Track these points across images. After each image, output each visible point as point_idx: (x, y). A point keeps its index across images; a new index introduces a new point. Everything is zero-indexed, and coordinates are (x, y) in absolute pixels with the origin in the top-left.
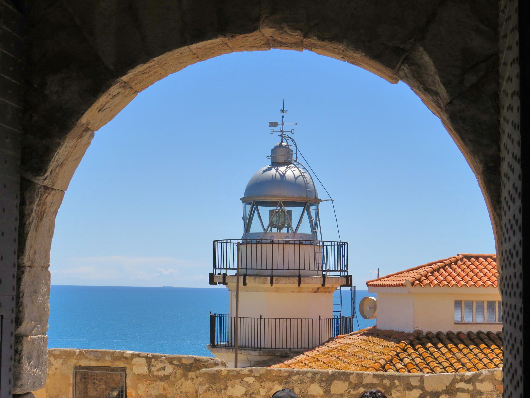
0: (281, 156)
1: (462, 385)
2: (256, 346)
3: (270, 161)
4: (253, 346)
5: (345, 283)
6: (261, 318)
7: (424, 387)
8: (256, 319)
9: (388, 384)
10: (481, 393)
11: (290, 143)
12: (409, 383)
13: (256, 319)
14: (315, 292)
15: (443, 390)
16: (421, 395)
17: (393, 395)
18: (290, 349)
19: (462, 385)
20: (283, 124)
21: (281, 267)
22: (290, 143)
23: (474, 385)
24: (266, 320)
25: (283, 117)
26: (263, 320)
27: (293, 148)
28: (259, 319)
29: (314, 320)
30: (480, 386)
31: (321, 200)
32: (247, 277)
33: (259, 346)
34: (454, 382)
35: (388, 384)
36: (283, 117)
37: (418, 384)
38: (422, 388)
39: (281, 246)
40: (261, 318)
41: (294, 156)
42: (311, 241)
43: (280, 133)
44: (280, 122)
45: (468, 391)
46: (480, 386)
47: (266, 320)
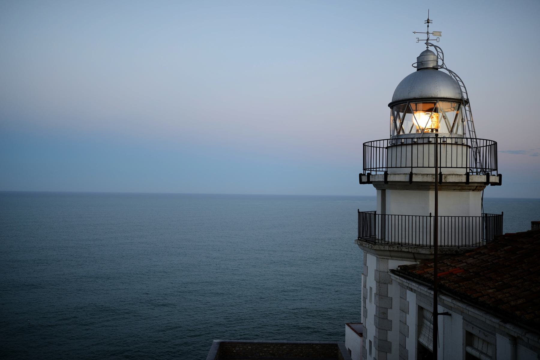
3: (416, 69)
8: (425, 218)
13: (425, 218)
14: (473, 190)
18: (459, 247)
21: (449, 165)
25: (428, 26)
32: (414, 175)
36: (428, 26)
40: (430, 216)
41: (440, 63)
43: (426, 41)
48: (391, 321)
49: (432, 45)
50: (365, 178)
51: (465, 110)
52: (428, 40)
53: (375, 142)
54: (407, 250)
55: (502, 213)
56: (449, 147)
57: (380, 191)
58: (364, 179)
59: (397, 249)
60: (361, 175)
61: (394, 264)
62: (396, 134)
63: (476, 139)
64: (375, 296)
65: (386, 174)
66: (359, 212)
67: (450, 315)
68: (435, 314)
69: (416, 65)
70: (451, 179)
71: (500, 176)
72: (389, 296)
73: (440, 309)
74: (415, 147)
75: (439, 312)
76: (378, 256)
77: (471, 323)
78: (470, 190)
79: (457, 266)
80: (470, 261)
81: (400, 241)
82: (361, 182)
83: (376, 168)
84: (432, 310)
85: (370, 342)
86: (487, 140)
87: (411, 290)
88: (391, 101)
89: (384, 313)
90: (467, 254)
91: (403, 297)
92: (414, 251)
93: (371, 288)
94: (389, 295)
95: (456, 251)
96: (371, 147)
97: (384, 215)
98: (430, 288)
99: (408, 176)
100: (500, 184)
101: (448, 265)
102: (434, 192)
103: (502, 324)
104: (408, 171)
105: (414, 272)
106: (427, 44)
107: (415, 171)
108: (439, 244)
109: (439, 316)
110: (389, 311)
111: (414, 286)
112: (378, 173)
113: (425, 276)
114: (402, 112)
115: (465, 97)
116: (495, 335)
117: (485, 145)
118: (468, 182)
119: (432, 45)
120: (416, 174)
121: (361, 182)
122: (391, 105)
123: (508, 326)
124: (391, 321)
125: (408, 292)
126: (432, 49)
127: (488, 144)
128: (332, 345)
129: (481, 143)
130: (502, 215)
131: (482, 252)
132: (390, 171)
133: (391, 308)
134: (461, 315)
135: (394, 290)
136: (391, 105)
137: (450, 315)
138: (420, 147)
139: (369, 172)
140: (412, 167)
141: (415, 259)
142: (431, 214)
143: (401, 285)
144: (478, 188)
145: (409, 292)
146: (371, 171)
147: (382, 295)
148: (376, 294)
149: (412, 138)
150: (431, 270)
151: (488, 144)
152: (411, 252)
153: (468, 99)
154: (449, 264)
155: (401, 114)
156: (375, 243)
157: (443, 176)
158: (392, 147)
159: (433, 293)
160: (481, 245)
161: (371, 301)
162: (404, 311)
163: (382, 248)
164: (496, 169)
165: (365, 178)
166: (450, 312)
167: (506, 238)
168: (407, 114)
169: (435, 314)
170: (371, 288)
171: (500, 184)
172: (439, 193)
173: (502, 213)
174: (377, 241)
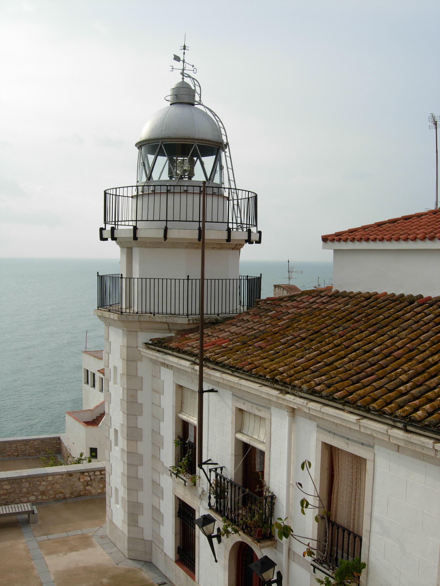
0: (184, 96)
2: (173, 312)
4: (169, 311)
6: (188, 279)
8: (182, 281)
13: (182, 281)
14: (233, 249)
20: (184, 61)
24: (194, 281)
26: (190, 281)
28: (186, 281)
32: (169, 231)
33: (185, 312)
40: (188, 279)
41: (197, 98)
43: (181, 71)
44: (182, 59)
47: (194, 281)
48: (142, 404)
49: (189, 76)
50: (108, 234)
51: (226, 156)
52: (183, 70)
53: (109, 190)
54: (160, 320)
55: (261, 275)
57: (125, 250)
58: (106, 234)
59: (148, 320)
60: (101, 230)
61: (145, 337)
62: (144, 179)
63: (236, 189)
64: (121, 377)
65: (135, 228)
66: (98, 275)
67: (217, 391)
68: (201, 392)
69: (169, 98)
71: (260, 233)
72: (138, 375)
73: (206, 387)
74: (170, 196)
75: (204, 389)
76: (125, 329)
77: (241, 398)
78: (229, 248)
79: (220, 336)
80: (233, 329)
81: (152, 311)
82: (102, 239)
83: (118, 221)
84: (196, 389)
85: (116, 431)
86: (249, 192)
87: (167, 366)
89: (132, 396)
90: (229, 322)
91: (156, 376)
92: (170, 320)
93: (115, 368)
94: (139, 374)
95: (216, 319)
96: (116, 195)
97: (130, 279)
98: (194, 363)
99: (162, 232)
100: (259, 242)
101: (209, 336)
102: (200, 251)
103: (281, 396)
105: (171, 345)
106: (183, 74)
108: (205, 312)
109: (205, 395)
110: (139, 393)
111: (172, 360)
112: (120, 227)
113: (186, 349)
114: (152, 153)
115: (225, 141)
116: (269, 409)
117: (247, 197)
118: (229, 240)
119: (189, 76)
121: (102, 239)
122: (140, 145)
123: (288, 397)
124: (142, 404)
125: (163, 369)
126: (187, 80)
127: (250, 196)
128: (54, 438)
129: (241, 195)
130: (261, 277)
131: (245, 318)
132: (140, 225)
133: (141, 389)
134: (230, 391)
135: (143, 369)
137: (217, 391)
138: (177, 197)
139: (114, 226)
140: (167, 221)
141: (170, 330)
142: (188, 276)
143: (154, 362)
144: (237, 247)
145: (163, 370)
146: (115, 224)
147: (131, 375)
148: (122, 374)
149: (167, 186)
150: (196, 344)
151: (250, 196)
152: (166, 323)
153: (227, 144)
154: (210, 334)
155: (151, 158)
156: (122, 313)
158: (137, 196)
159: (197, 367)
160: (242, 312)
161: (115, 383)
162: (158, 391)
163: (131, 318)
164: (256, 226)
165: (108, 234)
166: (216, 388)
167: (268, 302)
168: (158, 157)
169: (201, 392)
170: (115, 368)
171: (259, 242)
173: (261, 275)
174: (124, 311)
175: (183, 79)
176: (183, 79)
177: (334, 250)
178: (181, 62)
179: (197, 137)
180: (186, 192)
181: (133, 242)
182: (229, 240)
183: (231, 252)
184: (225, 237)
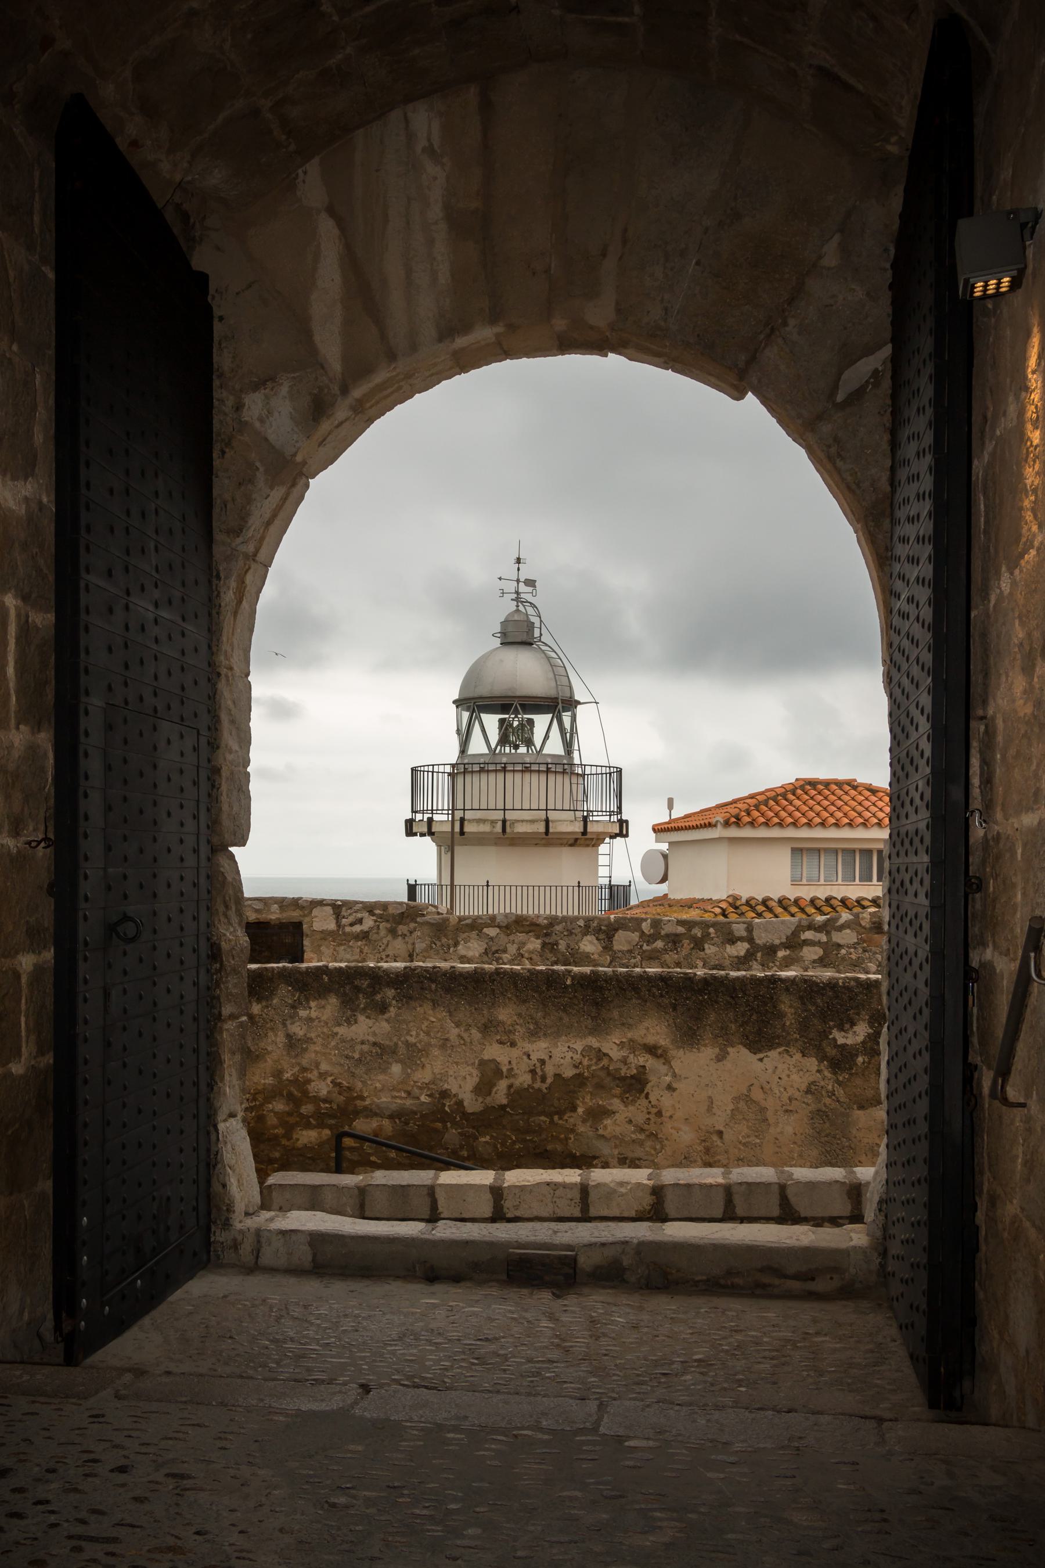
0: (518, 634)
1: (808, 935)
3: (499, 641)
5: (618, 831)
7: (753, 939)
9: (699, 935)
10: (839, 946)
11: (530, 611)
12: (731, 932)
14: (571, 845)
15: (782, 943)
16: (748, 950)
17: (707, 951)
19: (808, 935)
20: (518, 581)
21: (518, 806)
22: (530, 611)
23: (828, 933)
27: (535, 620)
29: (570, 889)
30: (837, 937)
31: (579, 703)
34: (800, 928)
35: (699, 935)
37: (744, 934)
38: (750, 940)
39: (518, 776)
40: (488, 886)
41: (537, 634)
42: (564, 767)
43: (514, 596)
45: (819, 943)
46: (837, 937)
56: (535, 777)
70: (520, 828)
88: (457, 697)
104: (499, 815)
107: (510, 816)
120: (469, 821)
122: (458, 703)
136: (458, 703)
157: (508, 824)
172: (457, 849)
175: (518, 606)
176: (518, 606)
177: (670, 843)
178: (522, 580)
179: (518, 694)
180: (504, 770)
181: (453, 840)
182: (585, 833)
183: (566, 851)
184: (542, 829)
